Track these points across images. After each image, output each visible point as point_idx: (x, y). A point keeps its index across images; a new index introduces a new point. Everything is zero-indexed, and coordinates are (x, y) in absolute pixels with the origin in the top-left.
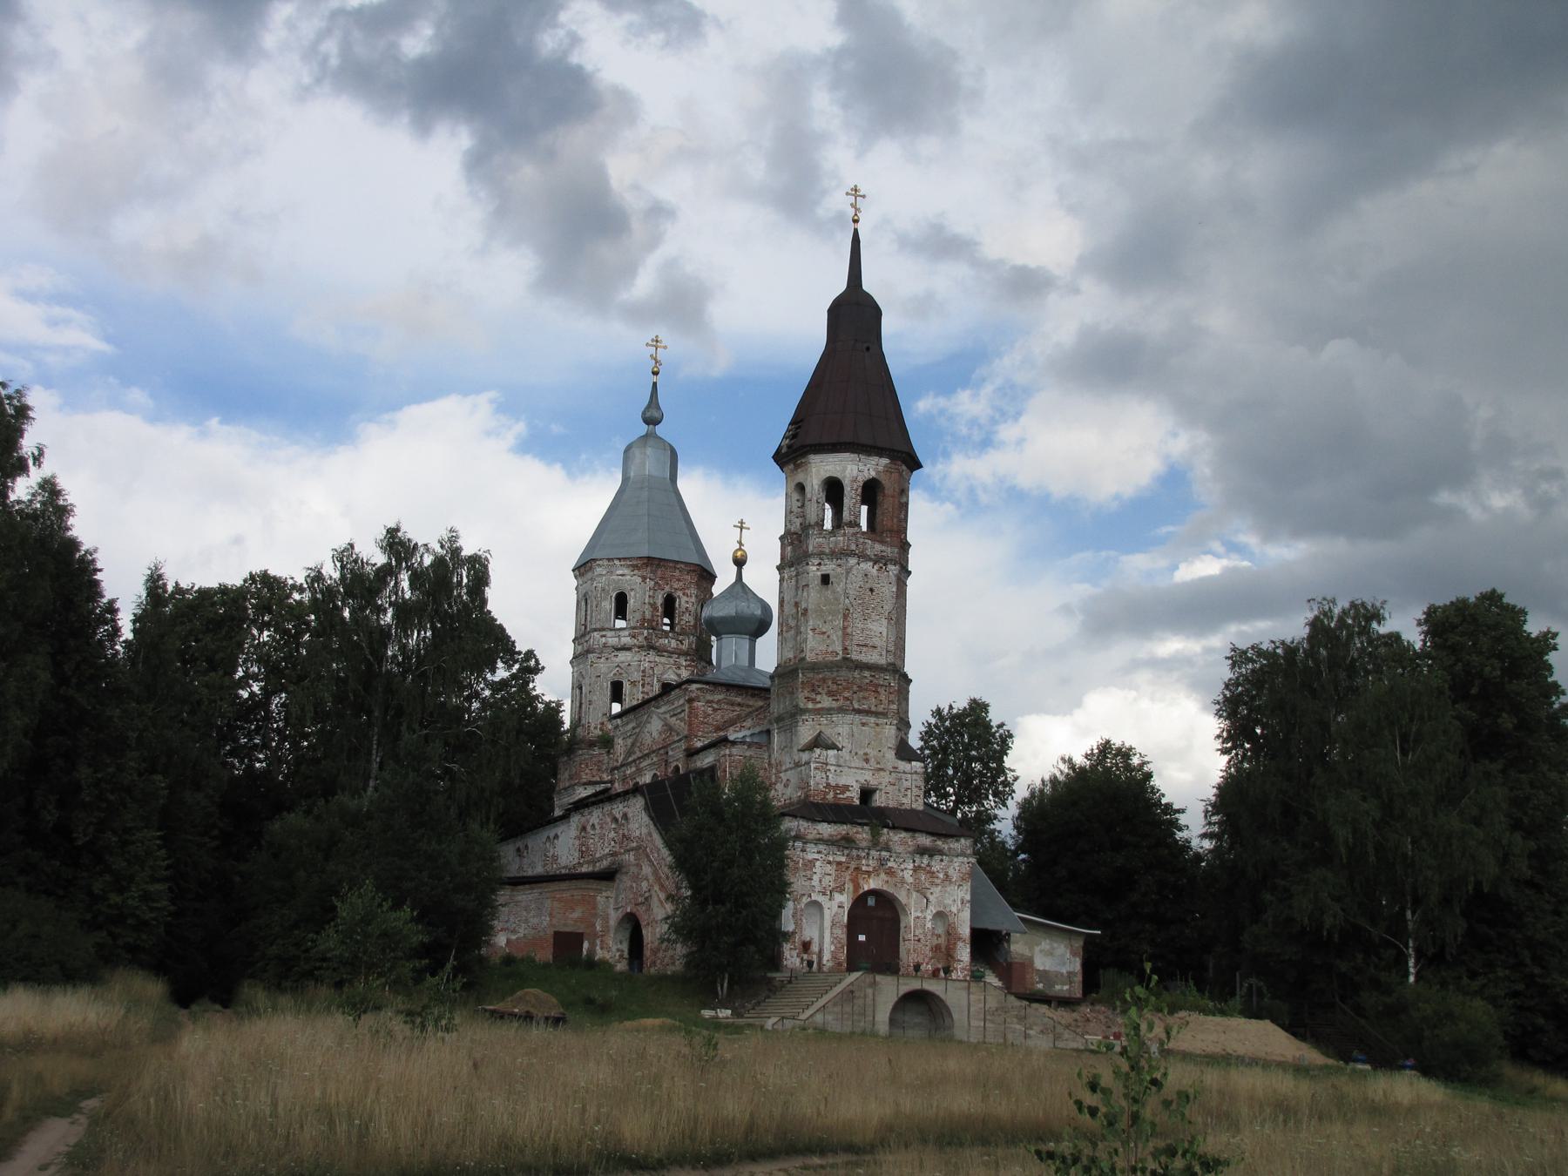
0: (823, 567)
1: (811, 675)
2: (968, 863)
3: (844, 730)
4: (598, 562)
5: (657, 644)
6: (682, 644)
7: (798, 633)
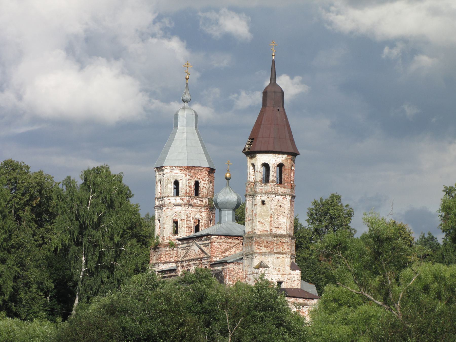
0: (262, 198)
1: (258, 239)
3: (271, 260)
4: (166, 168)
5: (192, 203)
7: (253, 222)
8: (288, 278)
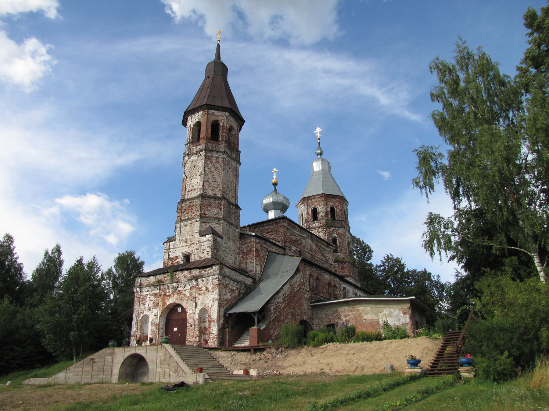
2: (216, 278)
6: (321, 224)
8: (197, 248)
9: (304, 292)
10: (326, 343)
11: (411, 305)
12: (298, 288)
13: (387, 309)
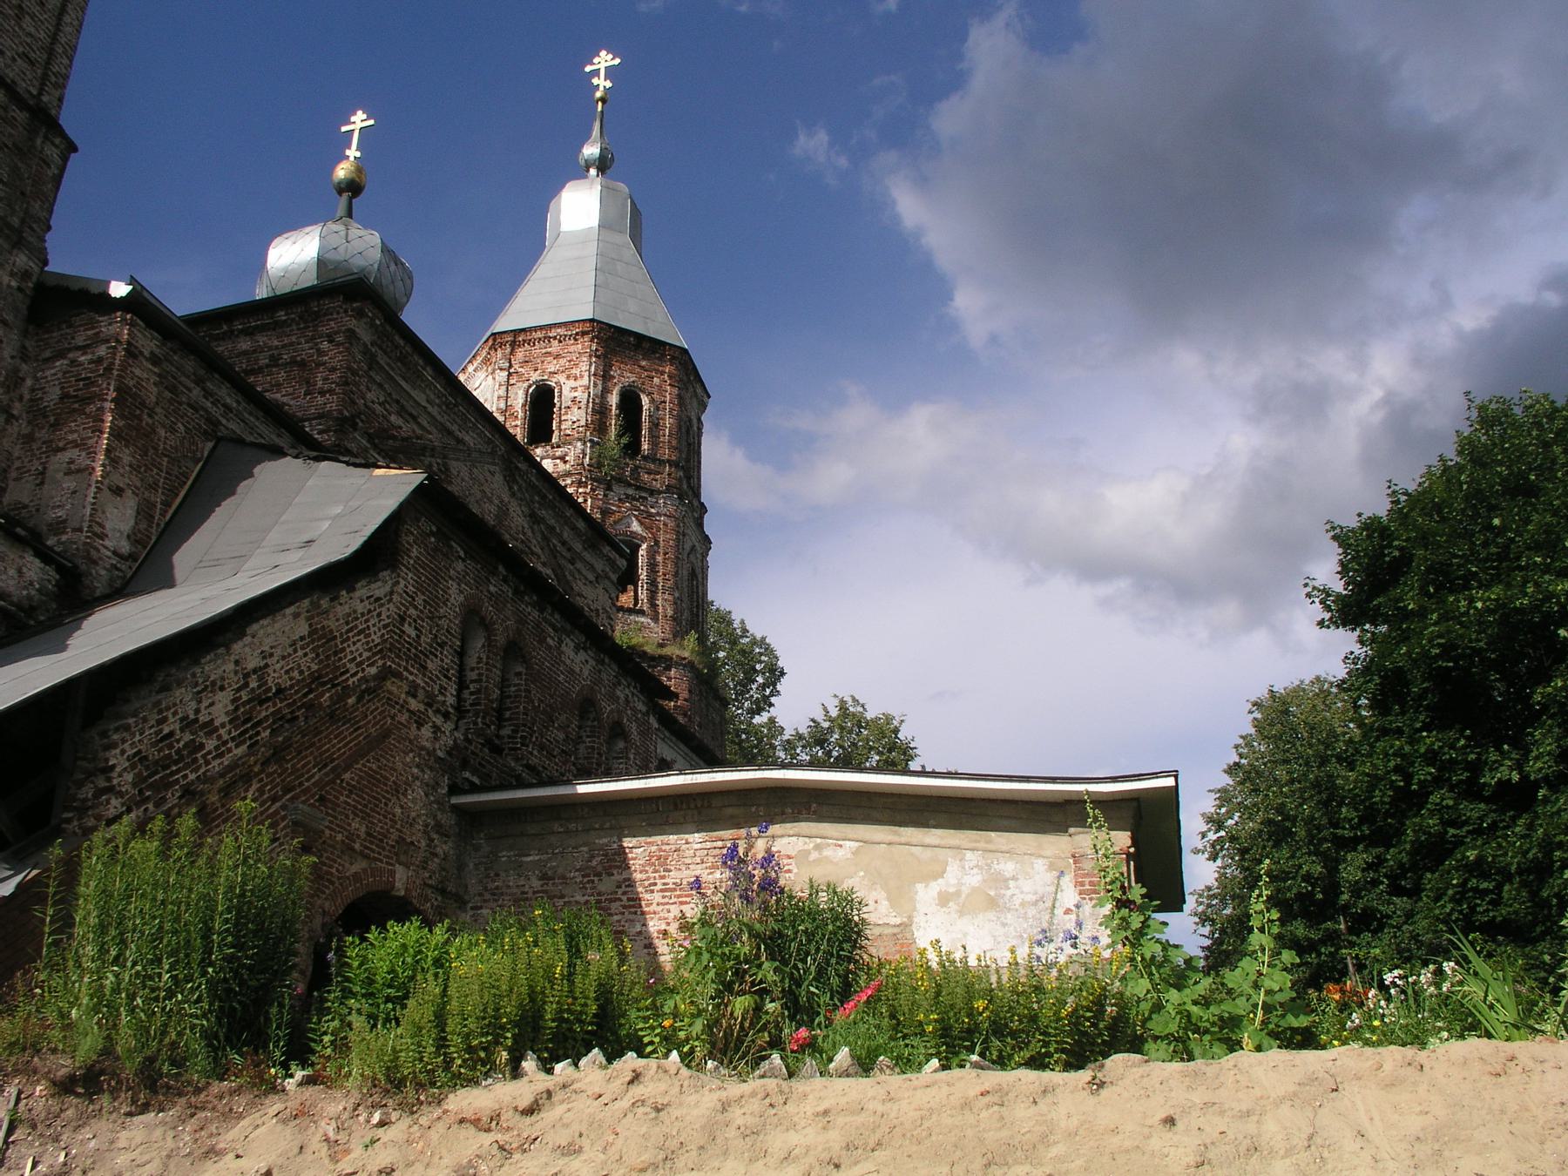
9: (414, 704)
10: (529, 1065)
11: (1135, 842)
12: (373, 670)
13: (969, 855)
